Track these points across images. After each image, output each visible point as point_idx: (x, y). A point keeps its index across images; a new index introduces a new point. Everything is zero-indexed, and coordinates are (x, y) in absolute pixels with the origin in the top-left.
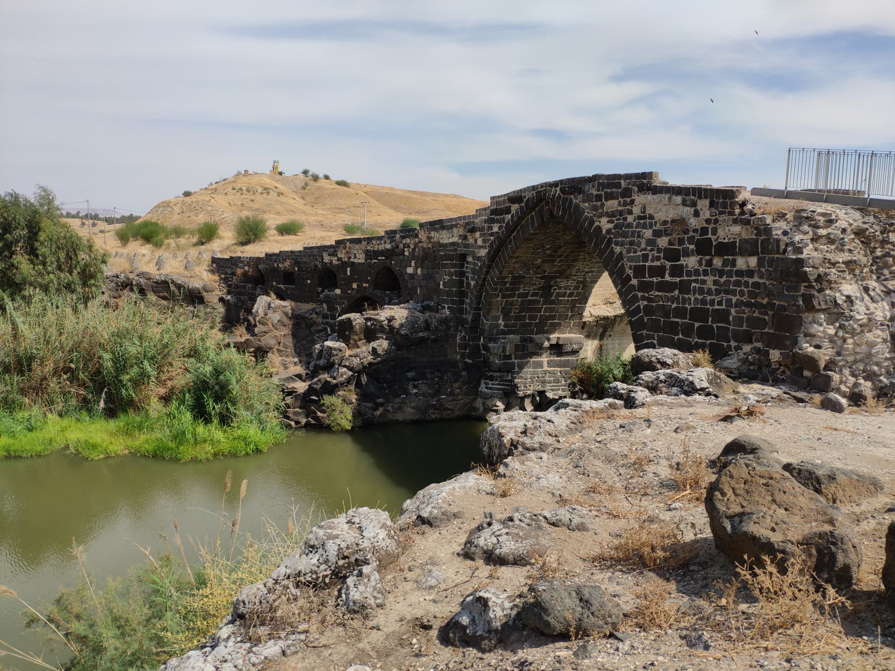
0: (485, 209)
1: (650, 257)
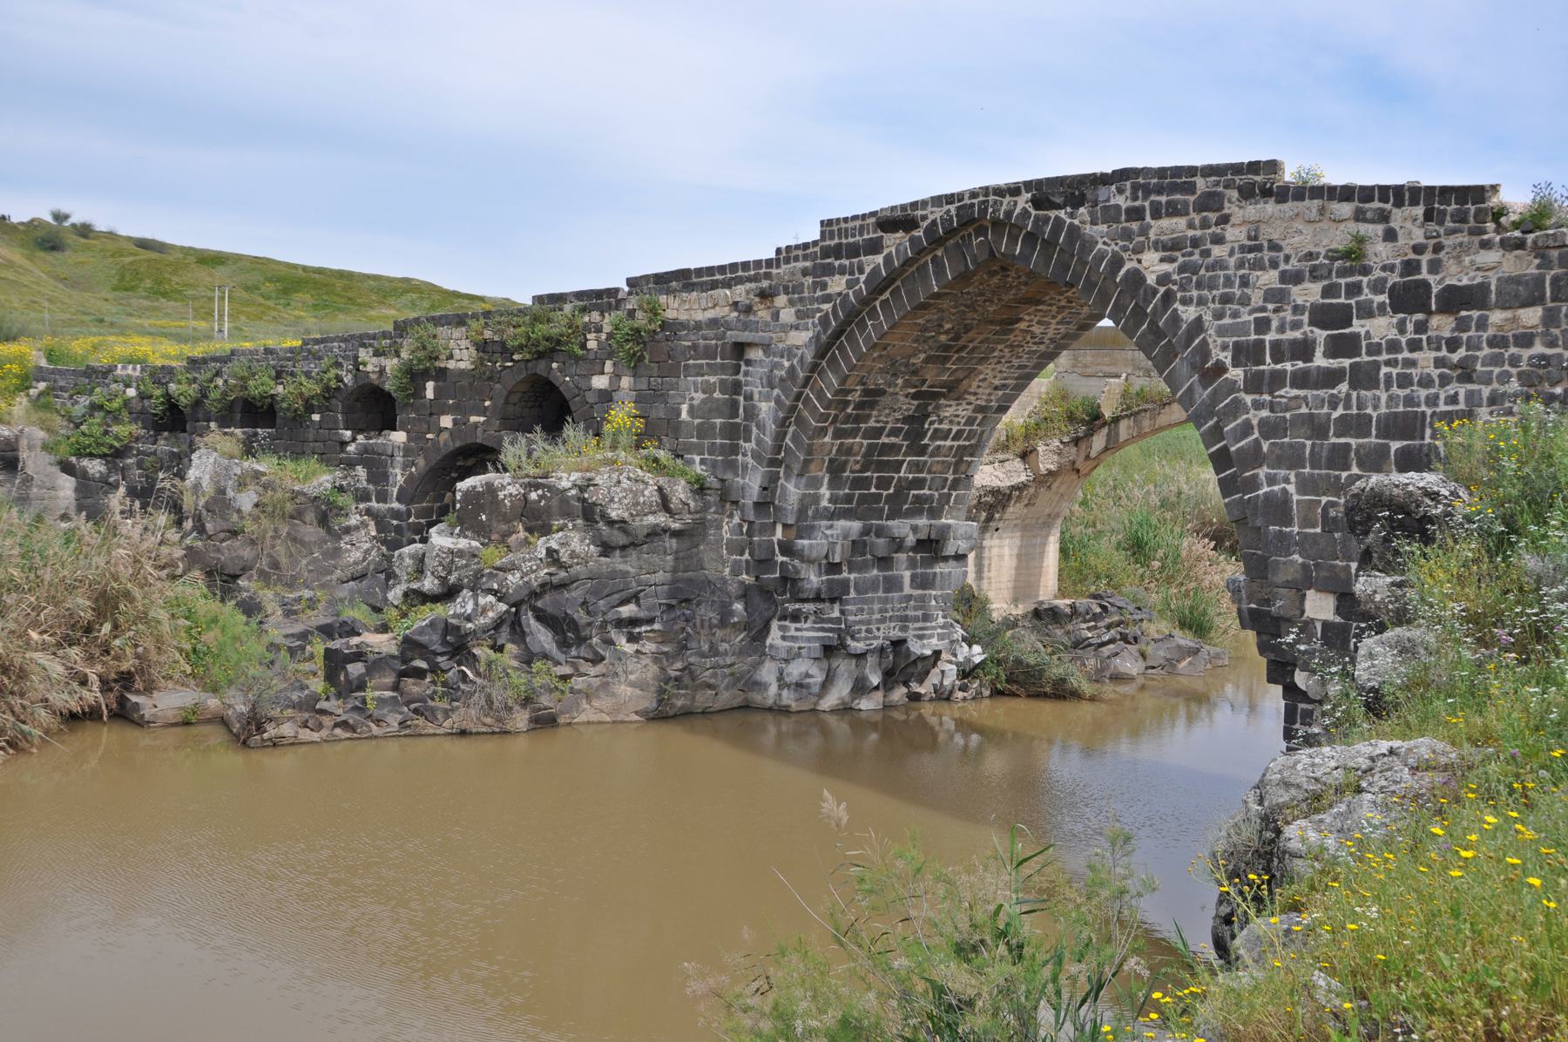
0: (806, 246)
1: (1274, 324)
